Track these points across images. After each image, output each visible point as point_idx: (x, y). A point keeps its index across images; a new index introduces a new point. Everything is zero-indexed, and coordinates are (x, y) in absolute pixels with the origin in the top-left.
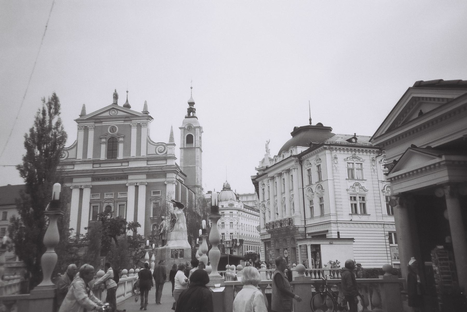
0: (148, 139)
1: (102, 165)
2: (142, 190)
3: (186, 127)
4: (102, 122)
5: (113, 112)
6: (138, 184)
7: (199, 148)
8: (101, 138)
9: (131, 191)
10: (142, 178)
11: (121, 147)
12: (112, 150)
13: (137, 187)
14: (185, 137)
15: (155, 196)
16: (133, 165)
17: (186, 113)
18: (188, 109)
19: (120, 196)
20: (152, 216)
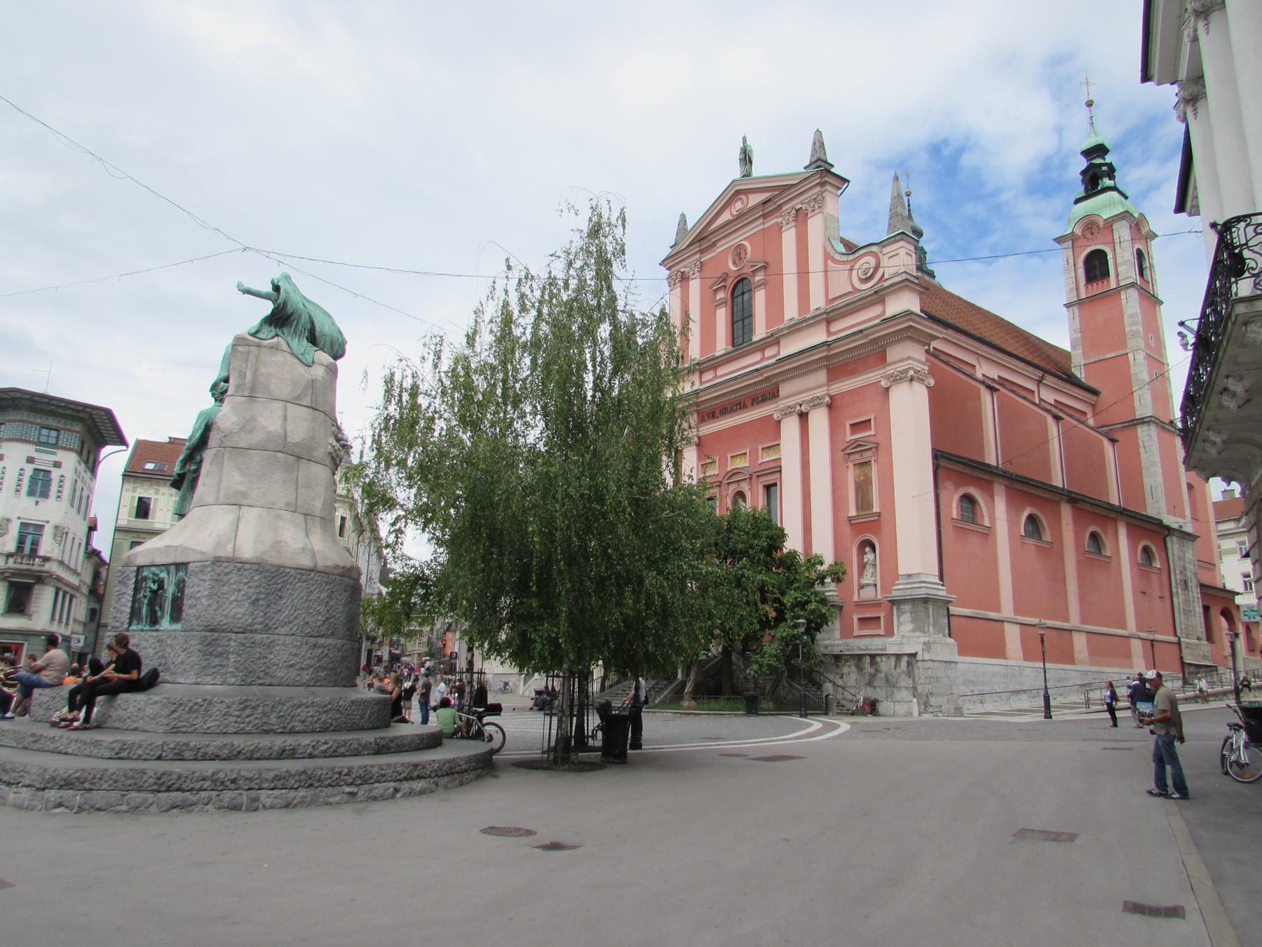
0: (829, 248)
1: (721, 371)
2: (819, 421)
3: (1078, 232)
4: (714, 244)
5: (739, 205)
6: (803, 408)
7: (1133, 285)
8: (716, 291)
9: (790, 428)
10: (816, 384)
11: (760, 298)
12: (743, 319)
13: (803, 416)
14: (1080, 264)
15: (856, 440)
16: (789, 347)
17: (1080, 190)
18: (1083, 173)
19: (766, 458)
20: (853, 513)
